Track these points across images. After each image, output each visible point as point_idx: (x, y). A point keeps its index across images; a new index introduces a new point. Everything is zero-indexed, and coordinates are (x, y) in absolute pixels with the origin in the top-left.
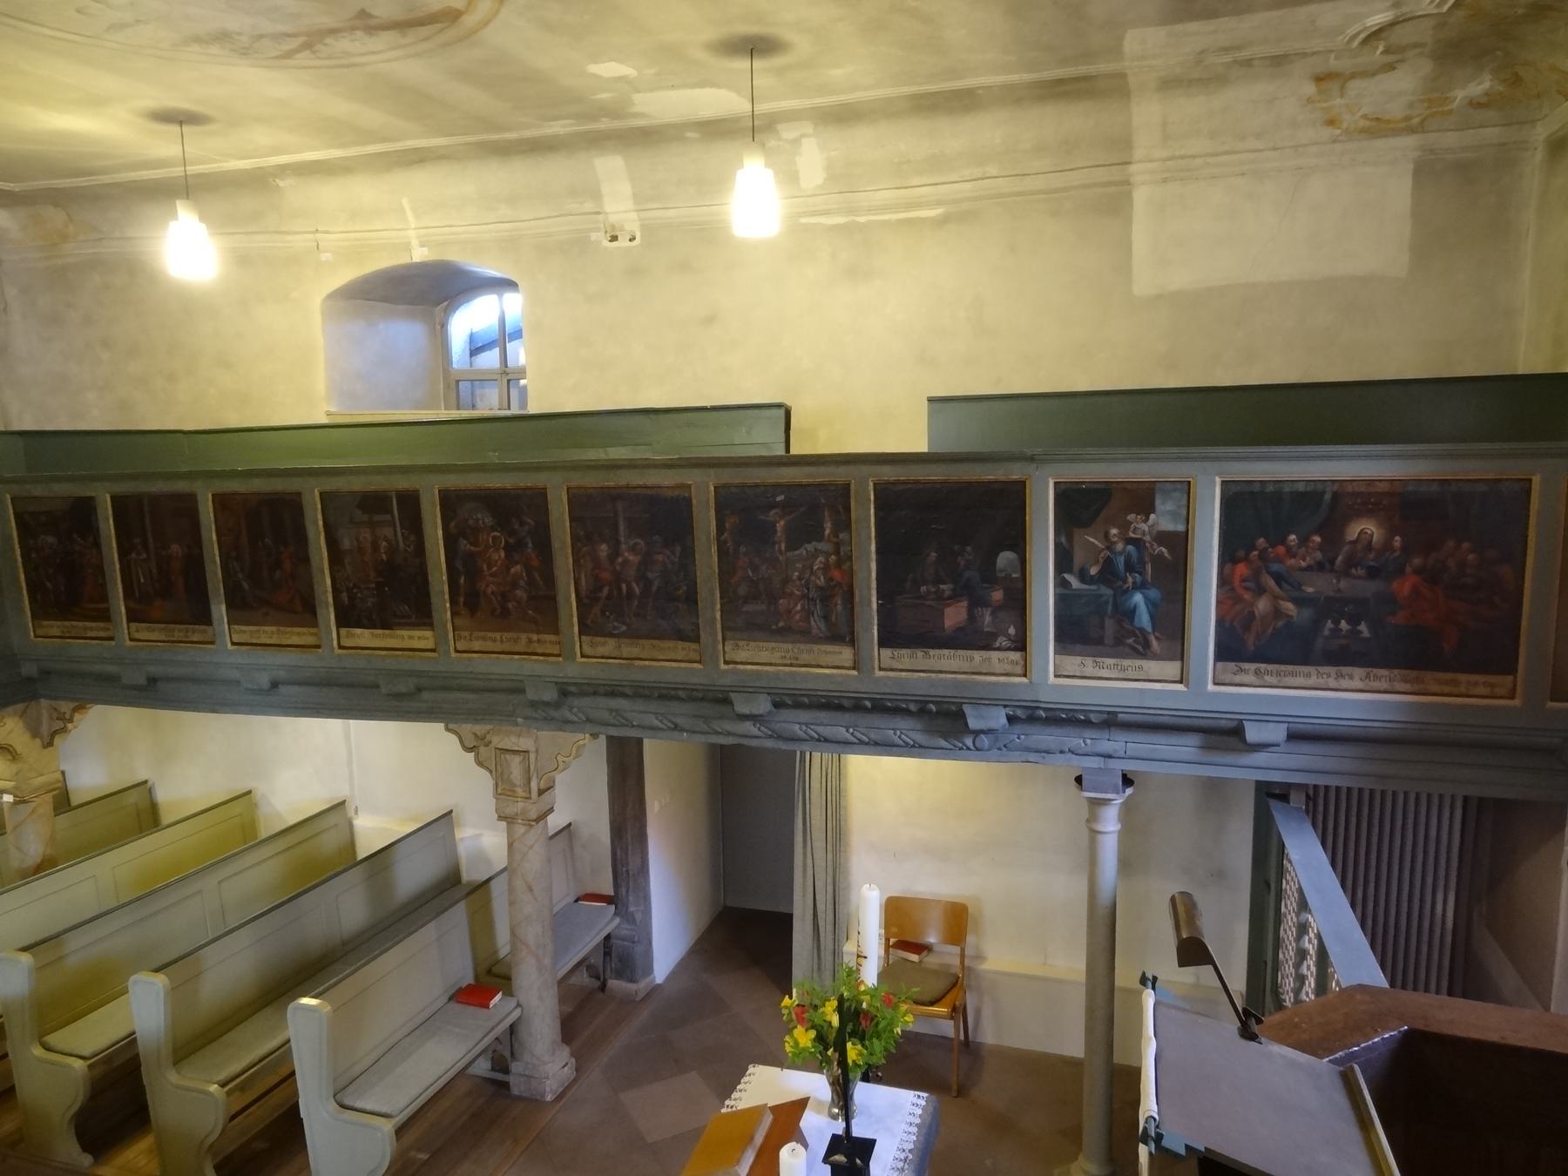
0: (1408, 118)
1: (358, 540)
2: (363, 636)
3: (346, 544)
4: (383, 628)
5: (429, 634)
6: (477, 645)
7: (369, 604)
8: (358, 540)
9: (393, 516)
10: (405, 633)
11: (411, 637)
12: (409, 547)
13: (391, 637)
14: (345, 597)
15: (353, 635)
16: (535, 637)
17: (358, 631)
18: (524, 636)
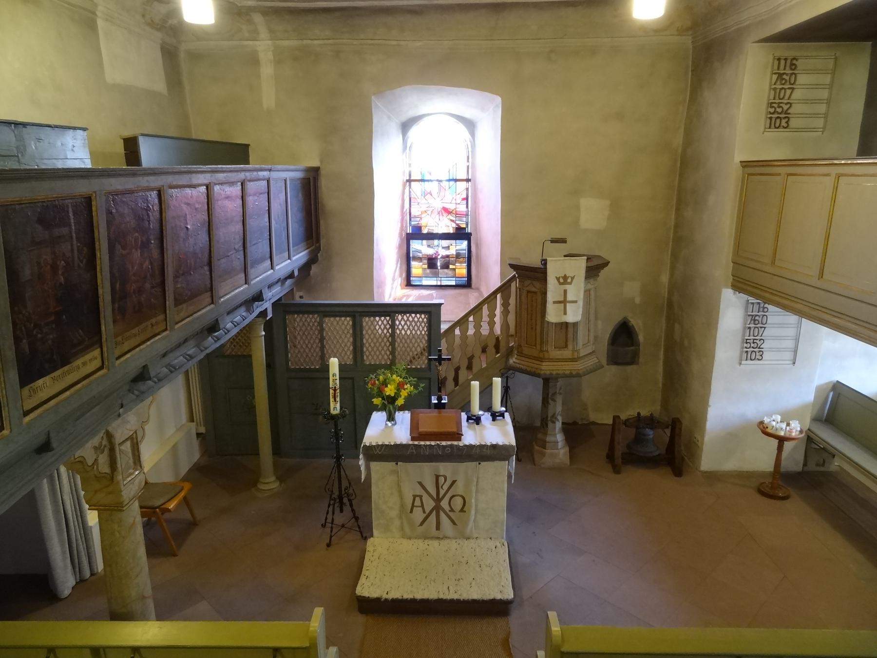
0: (158, 25)
1: (38, 263)
2: (46, 386)
3: (27, 273)
4: (64, 365)
5: (96, 352)
6: (126, 346)
7: (50, 342)
8: (38, 263)
9: (71, 228)
10: (79, 362)
11: (84, 364)
12: (82, 263)
13: (70, 372)
14: (25, 344)
15: (35, 391)
16: (154, 320)
17: (40, 382)
18: (149, 323)
